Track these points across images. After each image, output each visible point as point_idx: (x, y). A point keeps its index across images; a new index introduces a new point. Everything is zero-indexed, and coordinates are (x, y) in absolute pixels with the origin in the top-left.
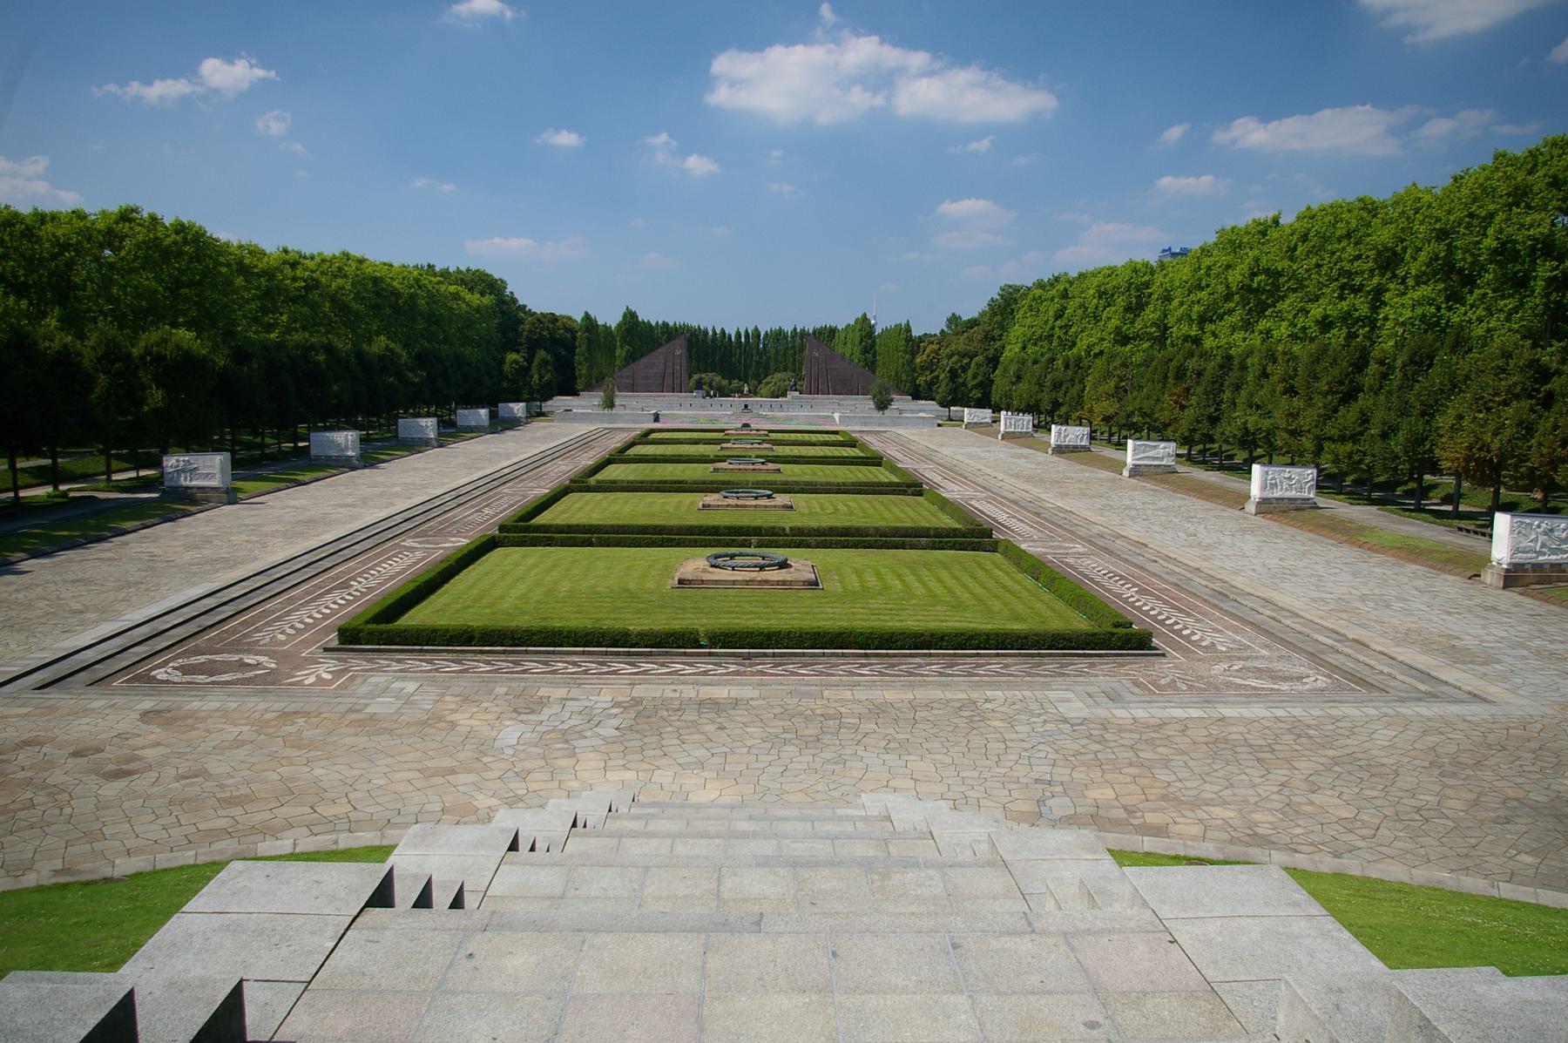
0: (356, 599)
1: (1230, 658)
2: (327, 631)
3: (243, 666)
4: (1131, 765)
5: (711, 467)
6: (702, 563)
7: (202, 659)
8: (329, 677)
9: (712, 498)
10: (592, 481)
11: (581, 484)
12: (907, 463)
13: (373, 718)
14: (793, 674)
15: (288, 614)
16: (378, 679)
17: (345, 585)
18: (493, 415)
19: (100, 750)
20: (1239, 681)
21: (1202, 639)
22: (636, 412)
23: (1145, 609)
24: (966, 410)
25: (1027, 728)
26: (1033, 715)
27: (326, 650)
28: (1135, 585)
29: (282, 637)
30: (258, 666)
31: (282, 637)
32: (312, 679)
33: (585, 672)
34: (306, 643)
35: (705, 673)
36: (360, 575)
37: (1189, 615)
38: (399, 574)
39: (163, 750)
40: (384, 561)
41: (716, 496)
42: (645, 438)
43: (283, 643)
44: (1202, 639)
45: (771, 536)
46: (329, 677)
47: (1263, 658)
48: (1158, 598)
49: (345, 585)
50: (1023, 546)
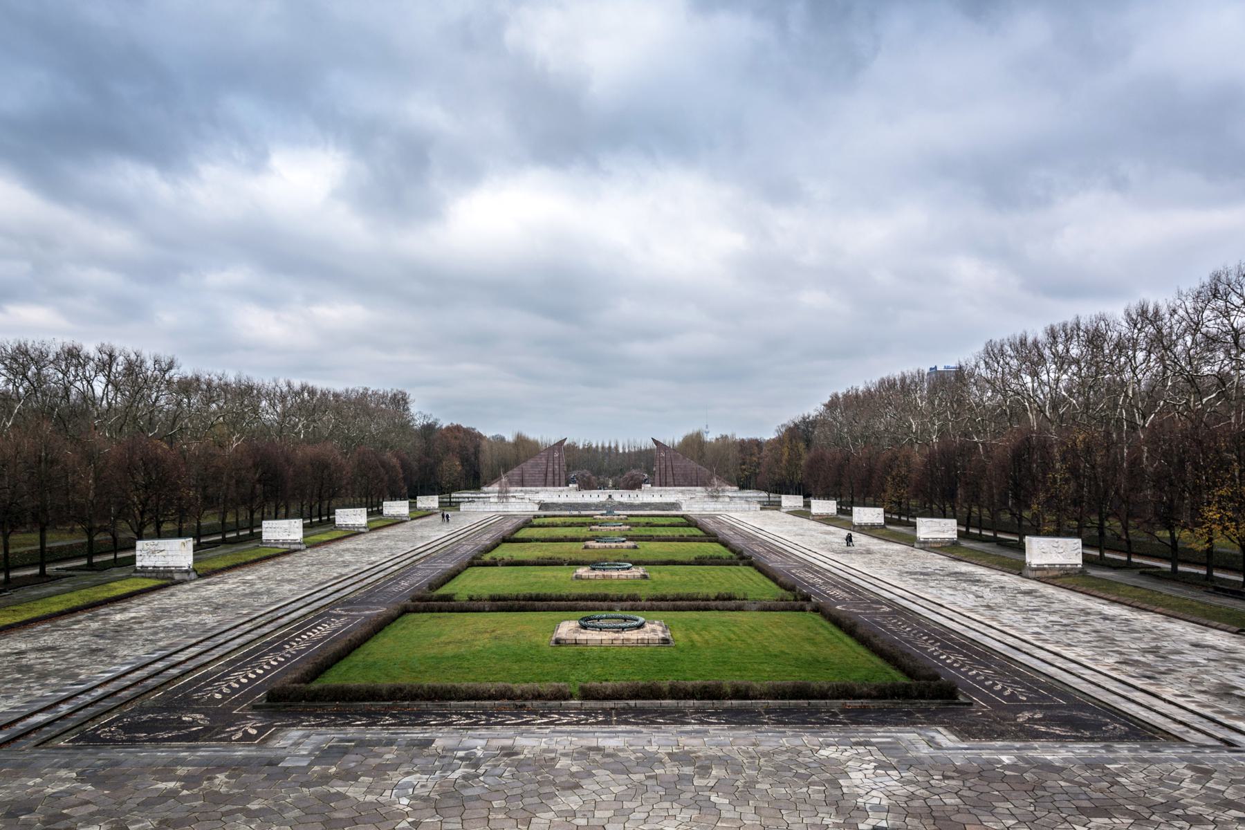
0: (287, 660)
1: (1032, 708)
2: (258, 690)
3: (182, 725)
4: (958, 811)
5: (582, 545)
6: (574, 624)
7: (144, 718)
8: (254, 732)
9: (583, 571)
10: (487, 557)
11: (475, 562)
12: (737, 541)
13: (287, 771)
14: (652, 723)
15: (228, 674)
16: (295, 734)
17: (280, 648)
18: (412, 506)
19: (30, 811)
20: (1043, 729)
21: (1004, 689)
22: (524, 502)
23: (950, 663)
24: (783, 497)
25: (860, 775)
26: (863, 762)
27: (255, 707)
28: (937, 640)
29: (218, 696)
30: (194, 723)
31: (218, 696)
32: (240, 734)
33: (475, 724)
34: (238, 702)
35: (578, 723)
36: (293, 639)
37: (988, 667)
38: (325, 638)
39: (92, 808)
40: (315, 627)
41: (586, 568)
42: (528, 524)
43: (220, 701)
44: (1004, 689)
45: (631, 602)
46: (254, 732)
47: (1061, 706)
48: (959, 652)
49: (280, 648)
50: (838, 607)
